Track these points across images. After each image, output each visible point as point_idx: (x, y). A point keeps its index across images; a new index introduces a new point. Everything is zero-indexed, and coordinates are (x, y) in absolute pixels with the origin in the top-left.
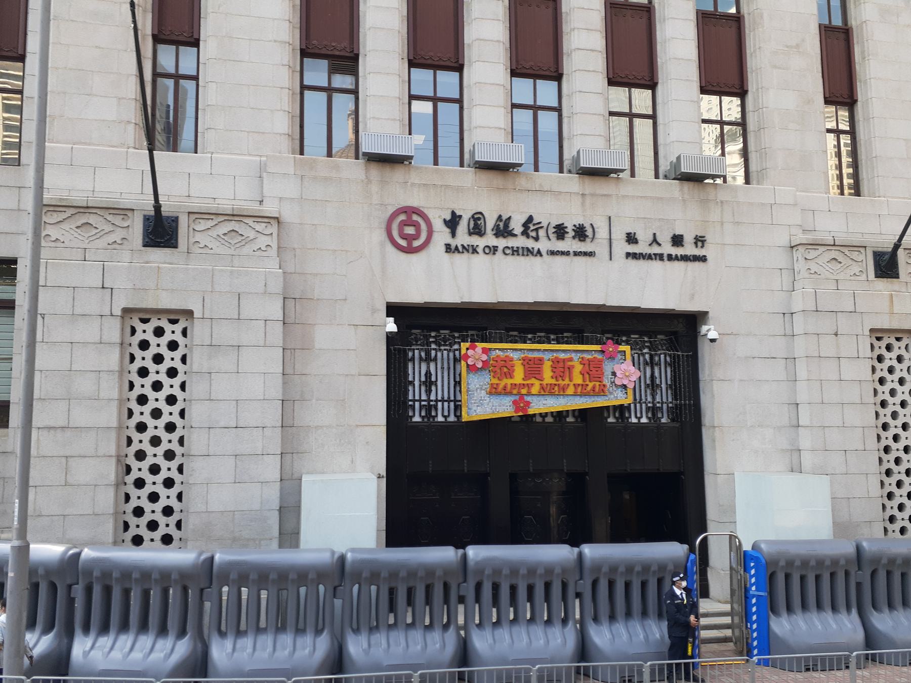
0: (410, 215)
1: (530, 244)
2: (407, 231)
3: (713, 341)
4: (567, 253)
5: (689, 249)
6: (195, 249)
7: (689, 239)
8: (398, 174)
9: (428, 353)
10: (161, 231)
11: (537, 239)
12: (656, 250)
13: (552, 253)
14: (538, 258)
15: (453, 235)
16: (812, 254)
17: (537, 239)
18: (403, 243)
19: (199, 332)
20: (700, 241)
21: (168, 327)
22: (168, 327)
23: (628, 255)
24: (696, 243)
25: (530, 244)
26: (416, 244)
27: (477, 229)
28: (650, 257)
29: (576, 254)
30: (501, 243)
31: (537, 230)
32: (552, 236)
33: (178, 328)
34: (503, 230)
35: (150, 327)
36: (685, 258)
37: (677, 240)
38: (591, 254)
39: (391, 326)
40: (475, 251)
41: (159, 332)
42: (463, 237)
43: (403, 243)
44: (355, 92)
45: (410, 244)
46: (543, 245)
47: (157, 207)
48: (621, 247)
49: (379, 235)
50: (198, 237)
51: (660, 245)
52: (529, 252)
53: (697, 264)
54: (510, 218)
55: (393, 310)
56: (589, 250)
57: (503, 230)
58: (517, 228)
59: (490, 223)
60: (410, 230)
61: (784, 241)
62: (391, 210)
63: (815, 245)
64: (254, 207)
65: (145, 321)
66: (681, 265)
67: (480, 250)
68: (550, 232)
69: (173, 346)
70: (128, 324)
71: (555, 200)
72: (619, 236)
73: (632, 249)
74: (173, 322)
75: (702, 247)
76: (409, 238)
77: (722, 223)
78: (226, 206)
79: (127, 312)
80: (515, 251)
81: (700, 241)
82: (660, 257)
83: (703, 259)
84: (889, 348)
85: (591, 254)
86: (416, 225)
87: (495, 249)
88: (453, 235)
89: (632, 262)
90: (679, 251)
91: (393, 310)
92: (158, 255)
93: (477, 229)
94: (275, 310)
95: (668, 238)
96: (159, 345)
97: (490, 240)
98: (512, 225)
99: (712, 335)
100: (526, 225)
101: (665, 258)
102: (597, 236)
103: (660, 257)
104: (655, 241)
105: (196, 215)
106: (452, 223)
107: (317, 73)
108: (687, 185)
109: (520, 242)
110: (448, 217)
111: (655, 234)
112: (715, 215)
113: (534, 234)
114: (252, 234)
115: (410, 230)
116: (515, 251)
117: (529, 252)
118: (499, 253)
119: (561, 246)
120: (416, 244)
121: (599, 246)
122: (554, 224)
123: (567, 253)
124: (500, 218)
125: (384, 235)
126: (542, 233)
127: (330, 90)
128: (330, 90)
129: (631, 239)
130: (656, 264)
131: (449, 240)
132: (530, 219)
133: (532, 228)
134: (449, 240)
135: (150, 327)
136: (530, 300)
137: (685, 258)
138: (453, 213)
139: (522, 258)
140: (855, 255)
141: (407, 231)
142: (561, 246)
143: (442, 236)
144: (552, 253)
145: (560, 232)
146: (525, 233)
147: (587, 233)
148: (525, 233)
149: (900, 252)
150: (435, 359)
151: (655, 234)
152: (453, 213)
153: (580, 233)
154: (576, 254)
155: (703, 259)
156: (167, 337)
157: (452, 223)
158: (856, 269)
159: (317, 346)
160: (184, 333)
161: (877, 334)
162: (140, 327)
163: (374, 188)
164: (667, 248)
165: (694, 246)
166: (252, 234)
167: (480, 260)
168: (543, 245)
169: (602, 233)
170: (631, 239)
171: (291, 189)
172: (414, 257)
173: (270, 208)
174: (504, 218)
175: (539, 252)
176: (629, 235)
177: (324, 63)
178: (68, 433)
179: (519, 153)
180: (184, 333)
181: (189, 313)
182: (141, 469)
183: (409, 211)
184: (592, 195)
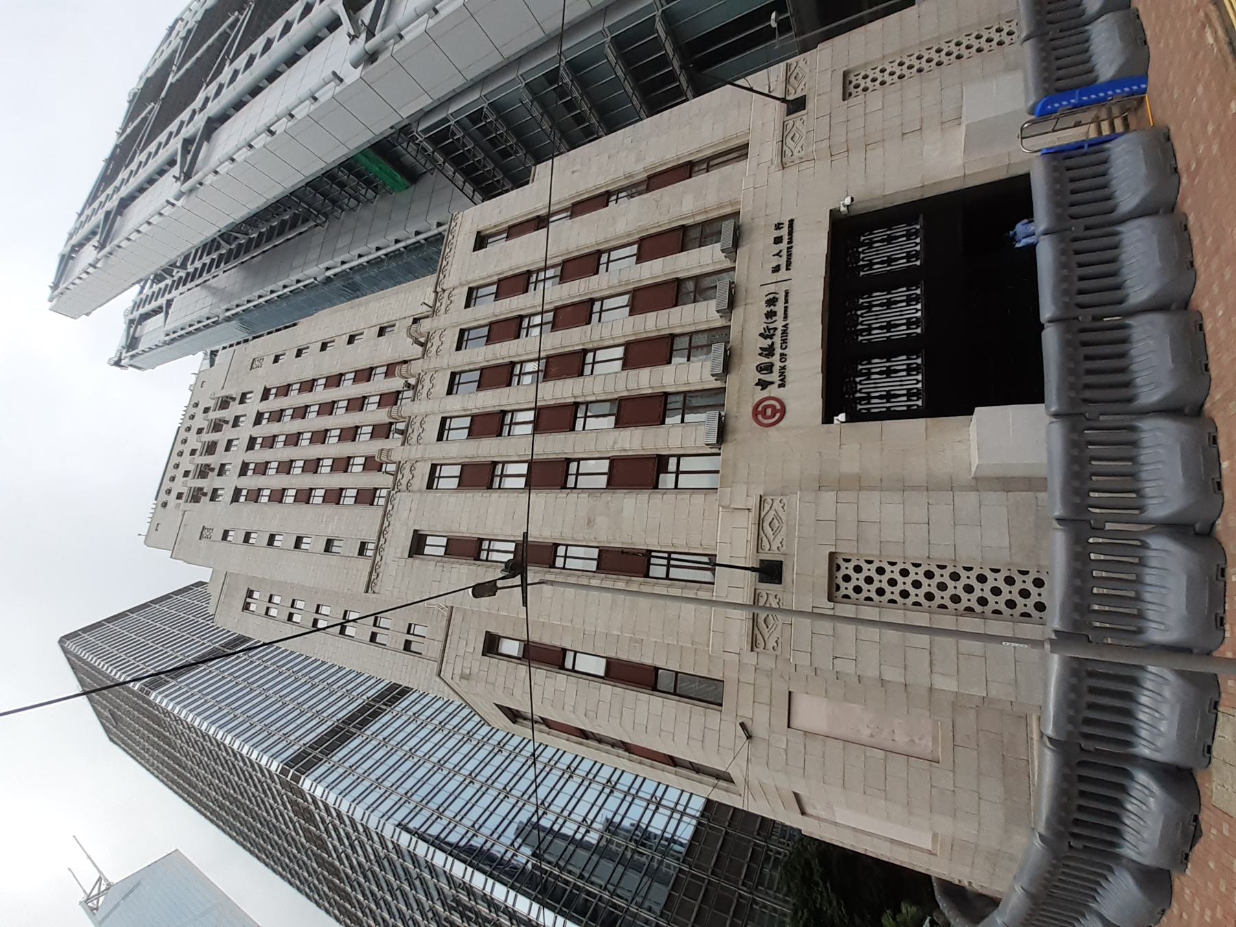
0: (759, 412)
1: (779, 333)
2: (770, 413)
3: (852, 199)
4: (786, 308)
5: (784, 232)
7: (777, 234)
8: (731, 423)
9: (862, 399)
10: (770, 572)
11: (775, 329)
12: (784, 253)
13: (786, 317)
15: (772, 383)
16: (788, 153)
17: (775, 329)
18: (778, 415)
19: (844, 549)
20: (778, 227)
21: (843, 572)
22: (843, 572)
23: (788, 269)
25: (779, 333)
26: (778, 407)
27: (769, 368)
29: (786, 302)
30: (778, 351)
33: (843, 565)
35: (843, 585)
36: (790, 233)
37: (778, 240)
38: (787, 293)
39: (842, 417)
40: (784, 368)
41: (847, 578)
42: (775, 377)
43: (778, 415)
44: (679, 457)
45: (778, 411)
46: (779, 324)
47: (752, 569)
48: (783, 274)
50: (774, 548)
52: (785, 332)
55: (828, 419)
56: (783, 294)
57: (769, 351)
58: (769, 342)
60: (769, 411)
63: (782, 153)
64: (753, 515)
65: (838, 588)
66: (795, 234)
69: (858, 569)
70: (839, 598)
71: (748, 325)
74: (839, 568)
78: (753, 529)
79: (830, 599)
80: (784, 341)
82: (789, 248)
83: (791, 222)
84: (857, 86)
85: (787, 293)
86: (765, 408)
87: (782, 355)
88: (772, 383)
90: (786, 240)
91: (828, 419)
92: (786, 575)
93: (769, 368)
94: (829, 497)
96: (858, 579)
98: (766, 346)
99: (848, 201)
103: (789, 248)
106: (763, 384)
107: (667, 480)
108: (742, 243)
109: (777, 339)
112: (761, 222)
114: (772, 513)
115: (769, 411)
116: (784, 341)
117: (785, 332)
120: (778, 407)
123: (786, 308)
125: (773, 428)
126: (771, 326)
127: (678, 473)
128: (678, 473)
129: (776, 269)
131: (776, 386)
132: (761, 335)
134: (776, 386)
135: (843, 585)
137: (790, 233)
139: (790, 336)
140: (789, 127)
141: (770, 413)
142: (781, 313)
143: (773, 391)
144: (786, 317)
146: (771, 337)
148: (771, 337)
149: (790, 98)
150: (868, 393)
153: (772, 302)
154: (786, 302)
155: (791, 222)
156: (851, 572)
157: (763, 384)
158: (798, 123)
159: (857, 470)
160: (847, 561)
161: (846, 95)
162: (843, 591)
163: (738, 436)
166: (772, 513)
169: (772, 288)
170: (776, 269)
171: (741, 490)
173: (753, 502)
175: (785, 326)
177: (662, 476)
178: (935, 650)
179: (719, 349)
180: (847, 561)
181: (832, 556)
182: (968, 600)
183: (755, 413)
184: (746, 299)
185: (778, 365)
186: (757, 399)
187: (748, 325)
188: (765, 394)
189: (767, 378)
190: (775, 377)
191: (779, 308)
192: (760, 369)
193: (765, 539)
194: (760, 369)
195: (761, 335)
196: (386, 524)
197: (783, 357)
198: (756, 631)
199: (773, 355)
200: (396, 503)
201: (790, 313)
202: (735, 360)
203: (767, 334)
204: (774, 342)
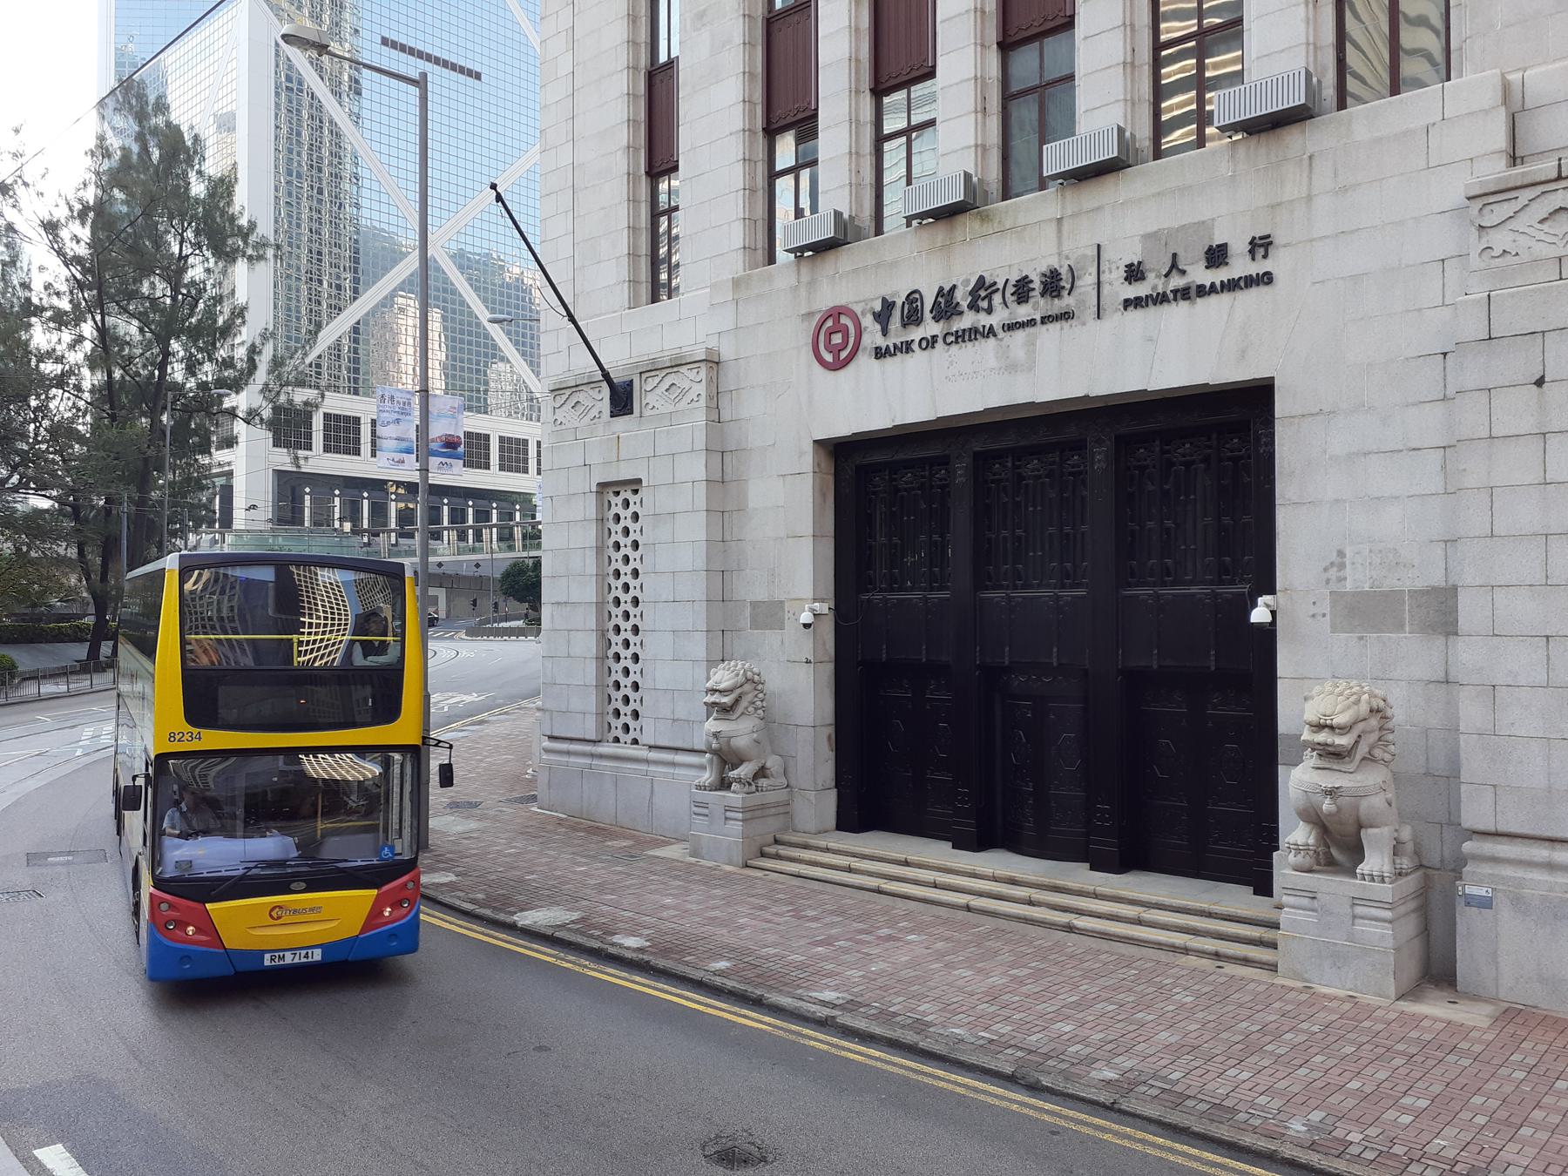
2: (835, 342)
6: (647, 412)
7: (1238, 246)
11: (989, 311)
12: (1177, 282)
13: (1011, 327)
14: (992, 340)
15: (885, 332)
16: (1506, 210)
17: (989, 311)
18: (829, 358)
23: (1127, 303)
24: (1252, 252)
25: (984, 320)
28: (1161, 299)
29: (1046, 320)
31: (989, 297)
32: (1010, 299)
34: (946, 307)
36: (1231, 286)
37: (1217, 256)
40: (907, 347)
43: (829, 358)
51: (1183, 272)
53: (1254, 293)
58: (964, 304)
59: (928, 303)
60: (837, 339)
61: (1453, 189)
62: (818, 317)
66: (1225, 298)
67: (915, 346)
68: (1008, 295)
75: (1265, 256)
77: (1309, 198)
81: (1261, 245)
82: (1184, 294)
83: (1266, 279)
85: (1066, 316)
87: (934, 338)
89: (1135, 315)
92: (622, 422)
93: (913, 317)
97: (931, 328)
100: (974, 293)
101: (1193, 292)
102: (1078, 283)
104: (1174, 267)
105: (652, 369)
106: (883, 317)
109: (967, 321)
110: (878, 307)
111: (1175, 255)
113: (985, 304)
114: (686, 384)
118: (940, 345)
119: (1023, 312)
120: (844, 355)
122: (1014, 278)
124: (941, 289)
126: (997, 298)
130: (1178, 311)
132: (982, 279)
133: (983, 293)
134: (881, 342)
136: (933, 418)
137: (1231, 286)
138: (884, 300)
141: (835, 342)
142: (1023, 312)
143: (873, 336)
145: (1022, 290)
146: (973, 306)
147: (1063, 283)
148: (973, 306)
151: (1175, 255)
152: (884, 300)
153: (1053, 284)
157: (883, 317)
164: (1200, 275)
165: (1248, 257)
167: (918, 357)
172: (841, 373)
174: (947, 288)
183: (836, 313)
185: (916, 334)
186: (858, 309)
188: (868, 321)
189: (897, 314)
190: (897, 335)
192: (913, 298)
193: (657, 380)
195: (982, 279)
197: (930, 343)
198: (568, 392)
199: (937, 319)
201: (1020, 335)
202: (940, 233)
203: (983, 291)
204: (948, 314)
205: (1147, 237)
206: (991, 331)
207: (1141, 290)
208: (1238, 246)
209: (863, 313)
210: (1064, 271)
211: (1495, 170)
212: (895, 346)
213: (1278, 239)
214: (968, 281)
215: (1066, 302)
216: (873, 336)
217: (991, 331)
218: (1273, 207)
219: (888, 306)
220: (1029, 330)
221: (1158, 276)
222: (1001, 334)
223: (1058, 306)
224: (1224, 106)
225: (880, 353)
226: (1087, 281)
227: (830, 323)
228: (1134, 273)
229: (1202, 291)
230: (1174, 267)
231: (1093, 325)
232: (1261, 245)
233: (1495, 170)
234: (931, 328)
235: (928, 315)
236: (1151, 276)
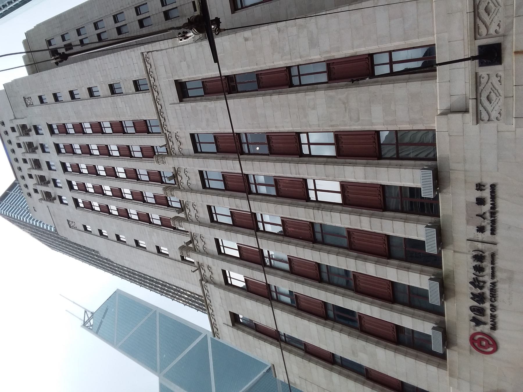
4: (493, 268)
5: (486, 194)
7: (479, 194)
11: (484, 282)
12: (488, 215)
13: (493, 276)
15: (485, 323)
24: (481, 190)
25: (488, 285)
28: (493, 222)
29: (493, 262)
34: (479, 298)
37: (480, 201)
40: (493, 317)
49: (487, 357)
51: (484, 213)
54: (472, 293)
59: (476, 304)
68: (479, 275)
72: (480, 236)
73: (488, 232)
76: (489, 345)
77: (465, 171)
81: (480, 187)
82: (493, 213)
83: (493, 187)
85: (493, 256)
86: (481, 339)
87: (491, 305)
93: (481, 311)
95: (478, 207)
97: (487, 305)
100: (476, 287)
106: (478, 323)
109: (487, 291)
110: (473, 324)
111: (477, 215)
118: (495, 304)
121: (488, 249)
122: (473, 271)
124: (472, 298)
126: (481, 279)
129: (481, 229)
132: (471, 283)
133: (477, 283)
142: (488, 271)
145: (479, 269)
146: (481, 288)
148: (481, 288)
151: (477, 215)
152: (471, 320)
153: (479, 258)
154: (493, 262)
157: (478, 323)
164: (486, 208)
167: (500, 314)
168: (487, 278)
174: (472, 296)
176: (478, 231)
183: (472, 340)
185: (488, 312)
186: (473, 332)
187: (458, 262)
188: (479, 329)
190: (487, 319)
191: (487, 264)
192: (473, 309)
194: (473, 309)
195: (471, 283)
196: (148, 66)
197: (493, 308)
200: (151, 61)
201: (498, 274)
203: (476, 283)
205: (468, 222)
206: (494, 284)
207: (488, 228)
208: (479, 194)
209: (475, 330)
210: (475, 253)
211: (469, 117)
212: (491, 321)
213: (478, 181)
214: (470, 288)
215: (487, 254)
216: (486, 329)
217: (494, 284)
218: (466, 182)
219: (474, 320)
220: (496, 269)
221: (484, 222)
222: (495, 280)
223: (488, 259)
224: (427, 193)
225: (494, 327)
226: (480, 246)
227: (476, 344)
228: (481, 229)
229: (494, 207)
230: (482, 216)
231: (499, 247)
232: (480, 187)
233: (469, 117)
234: (487, 305)
235: (481, 306)
236: (483, 224)
